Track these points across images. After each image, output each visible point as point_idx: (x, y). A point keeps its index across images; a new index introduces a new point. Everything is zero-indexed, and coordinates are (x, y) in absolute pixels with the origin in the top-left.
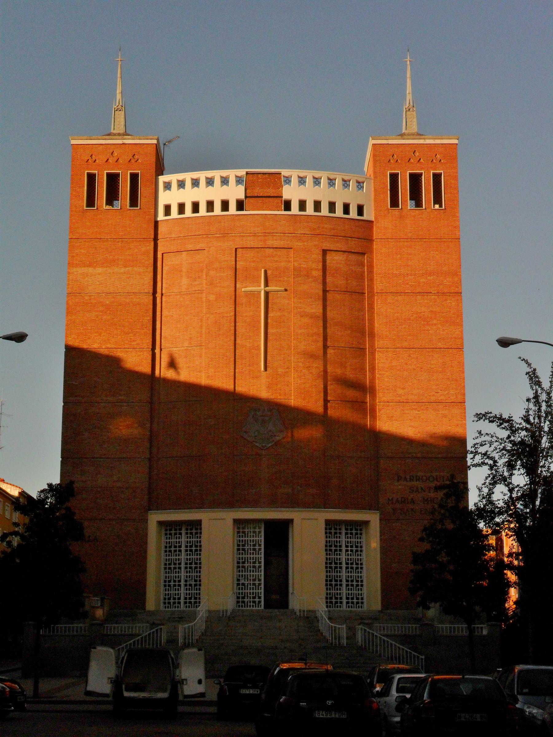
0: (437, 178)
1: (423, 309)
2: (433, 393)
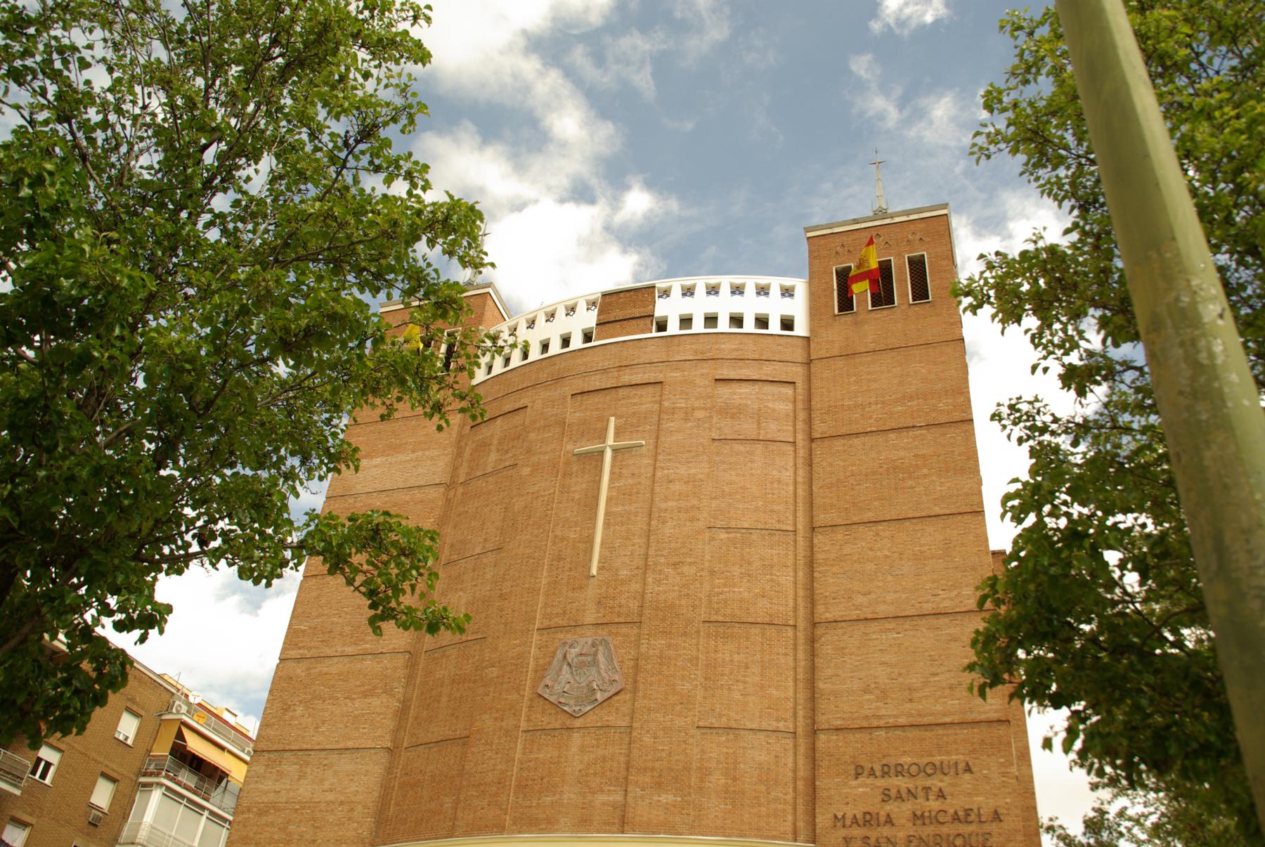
0: (917, 266)
1: (902, 453)
2: (929, 597)
